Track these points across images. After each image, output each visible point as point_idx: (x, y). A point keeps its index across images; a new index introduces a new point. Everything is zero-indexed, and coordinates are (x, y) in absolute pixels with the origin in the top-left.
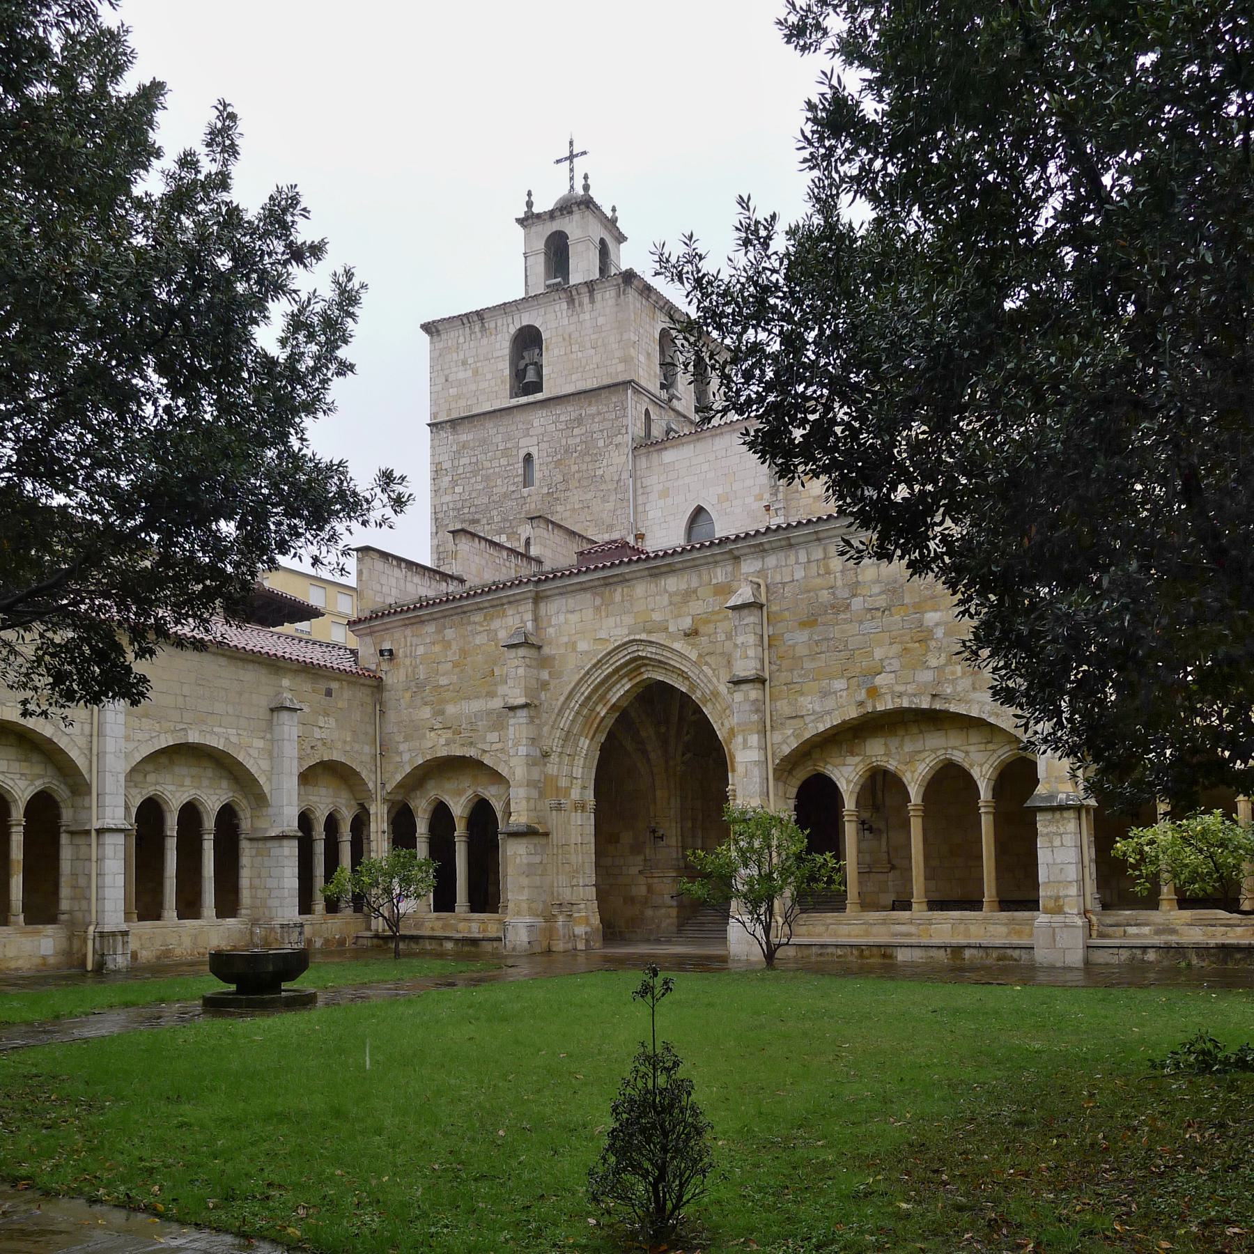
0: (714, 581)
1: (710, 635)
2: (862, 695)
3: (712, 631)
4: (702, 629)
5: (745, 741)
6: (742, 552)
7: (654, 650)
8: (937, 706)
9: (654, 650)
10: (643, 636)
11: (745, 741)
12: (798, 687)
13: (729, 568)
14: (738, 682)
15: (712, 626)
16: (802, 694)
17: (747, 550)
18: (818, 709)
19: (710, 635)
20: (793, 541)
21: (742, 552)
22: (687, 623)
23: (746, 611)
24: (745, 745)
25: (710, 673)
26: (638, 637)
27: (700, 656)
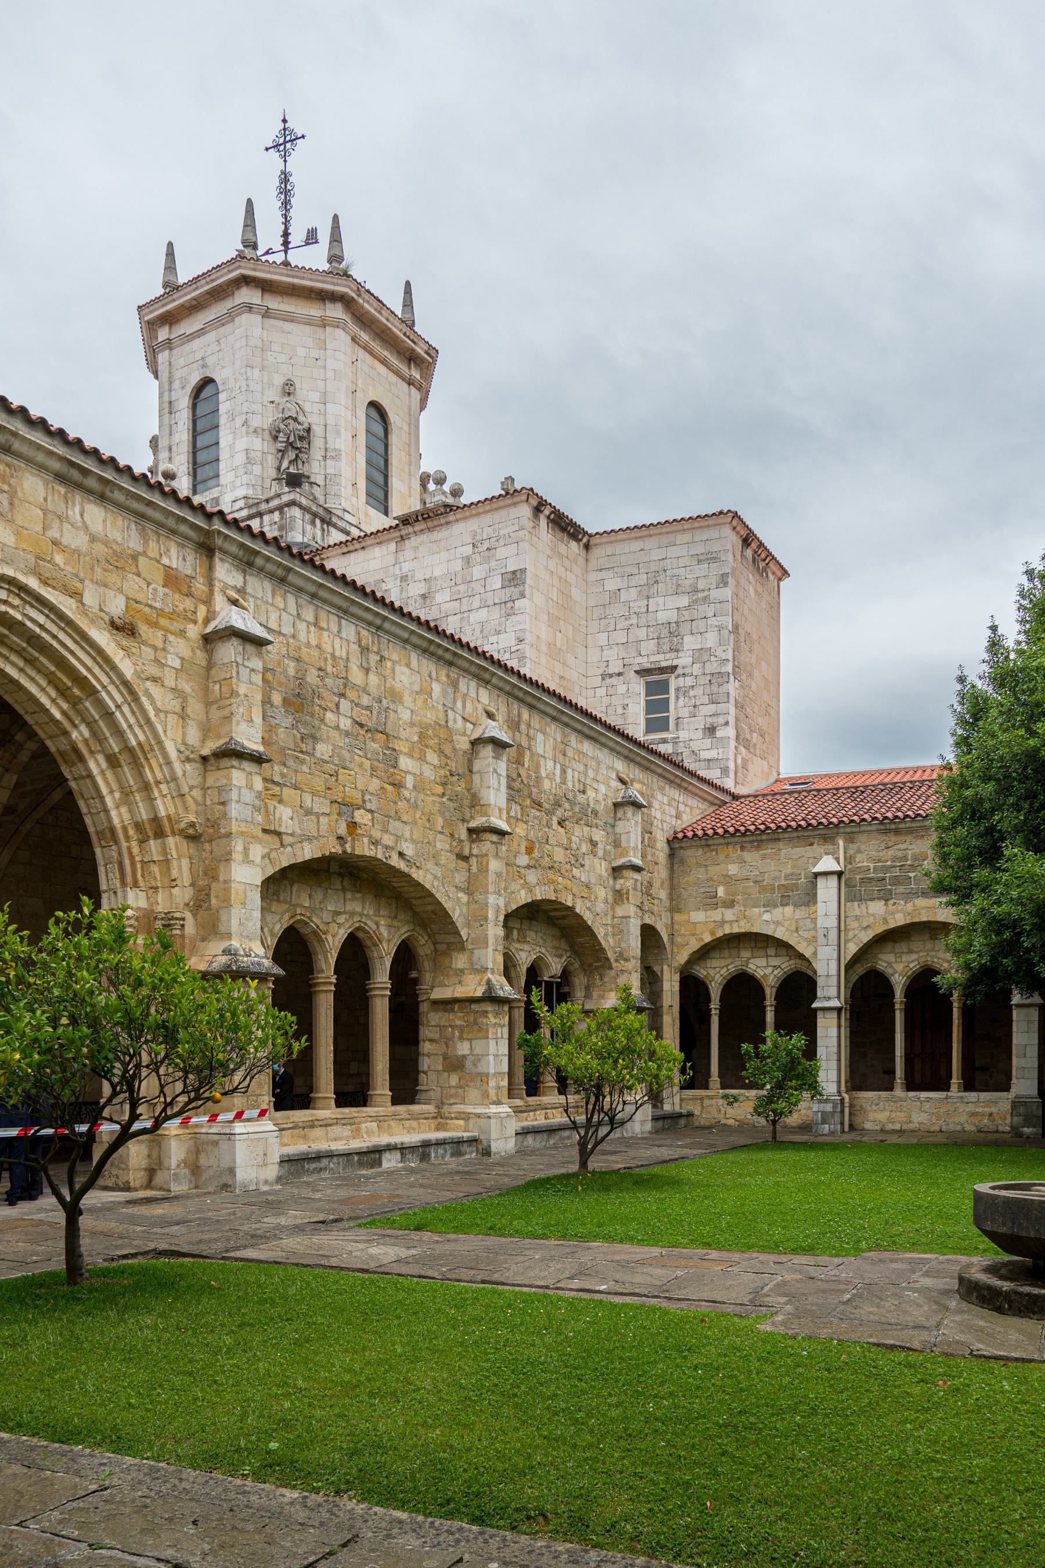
0: (165, 561)
1: (155, 648)
2: (342, 830)
3: (160, 644)
4: (143, 628)
5: (246, 850)
6: (227, 546)
7: (41, 619)
8: (402, 865)
9: (41, 619)
10: (33, 583)
11: (246, 850)
12: (276, 789)
13: (191, 556)
14: (233, 753)
15: (160, 633)
16: (280, 802)
17: (234, 549)
18: (298, 831)
19: (155, 648)
20: (291, 578)
21: (227, 546)
22: (117, 606)
23: (250, 648)
24: (247, 860)
25: (152, 714)
26: (22, 578)
27: (137, 674)
